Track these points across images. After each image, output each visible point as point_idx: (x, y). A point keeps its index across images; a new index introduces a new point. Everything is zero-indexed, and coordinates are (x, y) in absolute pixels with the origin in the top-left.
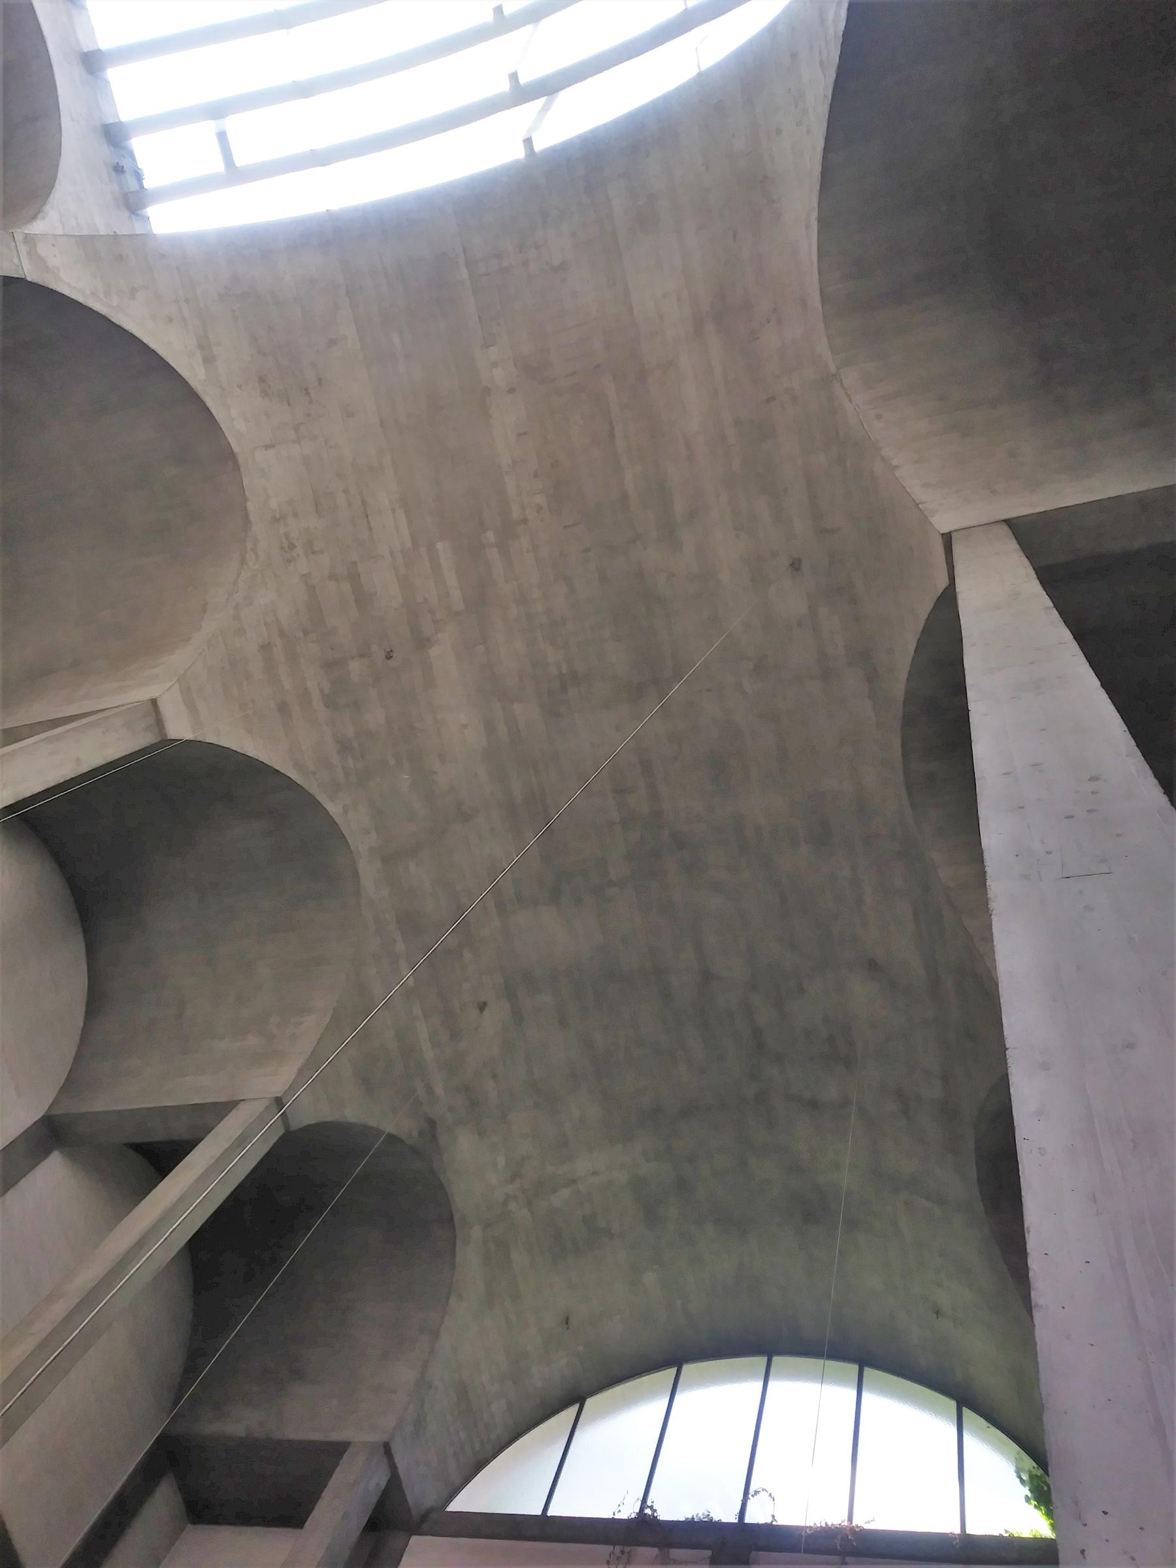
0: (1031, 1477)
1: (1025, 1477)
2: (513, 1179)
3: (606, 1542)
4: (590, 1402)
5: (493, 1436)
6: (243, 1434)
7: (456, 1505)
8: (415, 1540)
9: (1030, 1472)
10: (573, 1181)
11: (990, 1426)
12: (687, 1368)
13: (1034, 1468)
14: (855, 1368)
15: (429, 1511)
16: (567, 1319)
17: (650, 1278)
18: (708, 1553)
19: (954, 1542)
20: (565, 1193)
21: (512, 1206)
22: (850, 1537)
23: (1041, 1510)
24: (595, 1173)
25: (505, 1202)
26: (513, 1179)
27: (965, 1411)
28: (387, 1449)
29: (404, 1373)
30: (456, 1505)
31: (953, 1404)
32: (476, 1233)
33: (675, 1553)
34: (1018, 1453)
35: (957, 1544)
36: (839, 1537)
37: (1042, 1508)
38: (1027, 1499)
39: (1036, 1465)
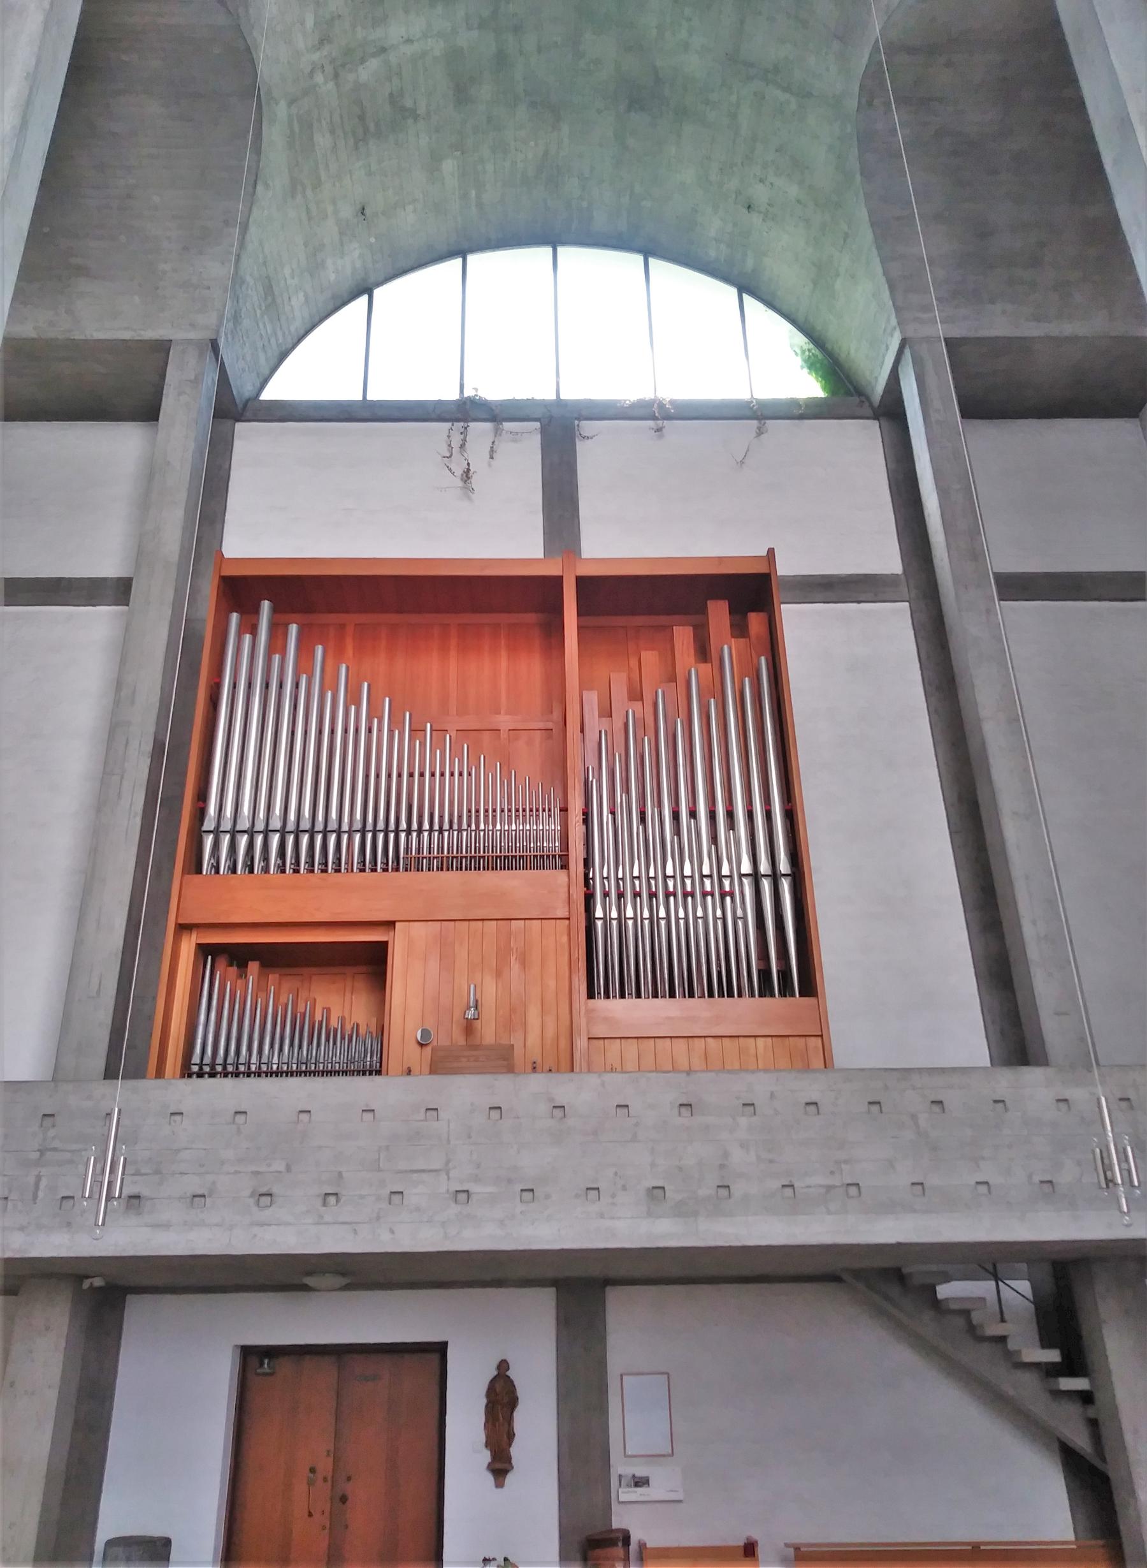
0: (803, 352)
1: (799, 352)
2: (322, 42)
3: (441, 419)
4: (378, 293)
5: (292, 329)
6: (34, 335)
7: (266, 395)
8: (239, 426)
9: (802, 347)
10: (383, 50)
11: (768, 309)
12: (471, 258)
13: (806, 343)
14: (640, 258)
15: (247, 401)
16: (364, 209)
17: (449, 166)
18: (537, 425)
19: (752, 405)
20: (374, 64)
21: (319, 78)
22: (667, 406)
23: (812, 375)
24: (409, 41)
25: (311, 74)
26: (322, 42)
27: (745, 297)
28: (214, 346)
29: (214, 269)
30: (266, 395)
31: (733, 291)
32: (281, 110)
33: (507, 425)
34: (790, 331)
35: (754, 406)
36: (656, 406)
37: (814, 374)
38: (802, 367)
39: (806, 340)
